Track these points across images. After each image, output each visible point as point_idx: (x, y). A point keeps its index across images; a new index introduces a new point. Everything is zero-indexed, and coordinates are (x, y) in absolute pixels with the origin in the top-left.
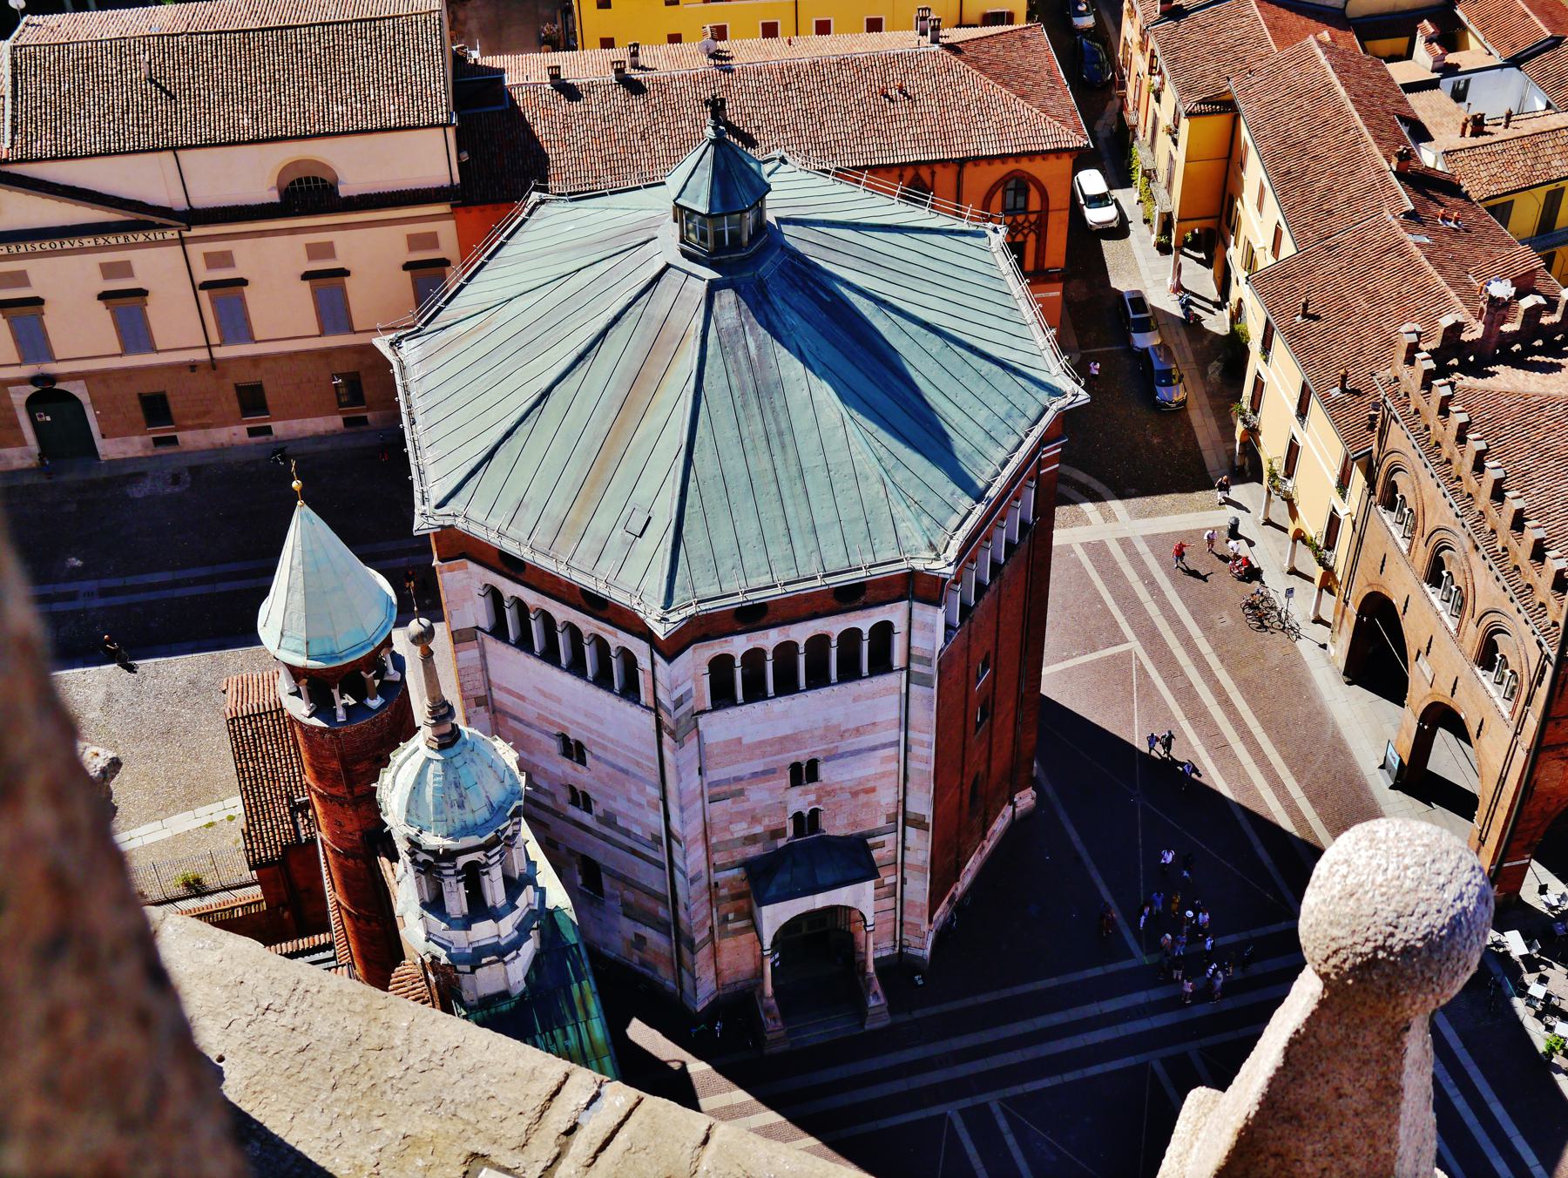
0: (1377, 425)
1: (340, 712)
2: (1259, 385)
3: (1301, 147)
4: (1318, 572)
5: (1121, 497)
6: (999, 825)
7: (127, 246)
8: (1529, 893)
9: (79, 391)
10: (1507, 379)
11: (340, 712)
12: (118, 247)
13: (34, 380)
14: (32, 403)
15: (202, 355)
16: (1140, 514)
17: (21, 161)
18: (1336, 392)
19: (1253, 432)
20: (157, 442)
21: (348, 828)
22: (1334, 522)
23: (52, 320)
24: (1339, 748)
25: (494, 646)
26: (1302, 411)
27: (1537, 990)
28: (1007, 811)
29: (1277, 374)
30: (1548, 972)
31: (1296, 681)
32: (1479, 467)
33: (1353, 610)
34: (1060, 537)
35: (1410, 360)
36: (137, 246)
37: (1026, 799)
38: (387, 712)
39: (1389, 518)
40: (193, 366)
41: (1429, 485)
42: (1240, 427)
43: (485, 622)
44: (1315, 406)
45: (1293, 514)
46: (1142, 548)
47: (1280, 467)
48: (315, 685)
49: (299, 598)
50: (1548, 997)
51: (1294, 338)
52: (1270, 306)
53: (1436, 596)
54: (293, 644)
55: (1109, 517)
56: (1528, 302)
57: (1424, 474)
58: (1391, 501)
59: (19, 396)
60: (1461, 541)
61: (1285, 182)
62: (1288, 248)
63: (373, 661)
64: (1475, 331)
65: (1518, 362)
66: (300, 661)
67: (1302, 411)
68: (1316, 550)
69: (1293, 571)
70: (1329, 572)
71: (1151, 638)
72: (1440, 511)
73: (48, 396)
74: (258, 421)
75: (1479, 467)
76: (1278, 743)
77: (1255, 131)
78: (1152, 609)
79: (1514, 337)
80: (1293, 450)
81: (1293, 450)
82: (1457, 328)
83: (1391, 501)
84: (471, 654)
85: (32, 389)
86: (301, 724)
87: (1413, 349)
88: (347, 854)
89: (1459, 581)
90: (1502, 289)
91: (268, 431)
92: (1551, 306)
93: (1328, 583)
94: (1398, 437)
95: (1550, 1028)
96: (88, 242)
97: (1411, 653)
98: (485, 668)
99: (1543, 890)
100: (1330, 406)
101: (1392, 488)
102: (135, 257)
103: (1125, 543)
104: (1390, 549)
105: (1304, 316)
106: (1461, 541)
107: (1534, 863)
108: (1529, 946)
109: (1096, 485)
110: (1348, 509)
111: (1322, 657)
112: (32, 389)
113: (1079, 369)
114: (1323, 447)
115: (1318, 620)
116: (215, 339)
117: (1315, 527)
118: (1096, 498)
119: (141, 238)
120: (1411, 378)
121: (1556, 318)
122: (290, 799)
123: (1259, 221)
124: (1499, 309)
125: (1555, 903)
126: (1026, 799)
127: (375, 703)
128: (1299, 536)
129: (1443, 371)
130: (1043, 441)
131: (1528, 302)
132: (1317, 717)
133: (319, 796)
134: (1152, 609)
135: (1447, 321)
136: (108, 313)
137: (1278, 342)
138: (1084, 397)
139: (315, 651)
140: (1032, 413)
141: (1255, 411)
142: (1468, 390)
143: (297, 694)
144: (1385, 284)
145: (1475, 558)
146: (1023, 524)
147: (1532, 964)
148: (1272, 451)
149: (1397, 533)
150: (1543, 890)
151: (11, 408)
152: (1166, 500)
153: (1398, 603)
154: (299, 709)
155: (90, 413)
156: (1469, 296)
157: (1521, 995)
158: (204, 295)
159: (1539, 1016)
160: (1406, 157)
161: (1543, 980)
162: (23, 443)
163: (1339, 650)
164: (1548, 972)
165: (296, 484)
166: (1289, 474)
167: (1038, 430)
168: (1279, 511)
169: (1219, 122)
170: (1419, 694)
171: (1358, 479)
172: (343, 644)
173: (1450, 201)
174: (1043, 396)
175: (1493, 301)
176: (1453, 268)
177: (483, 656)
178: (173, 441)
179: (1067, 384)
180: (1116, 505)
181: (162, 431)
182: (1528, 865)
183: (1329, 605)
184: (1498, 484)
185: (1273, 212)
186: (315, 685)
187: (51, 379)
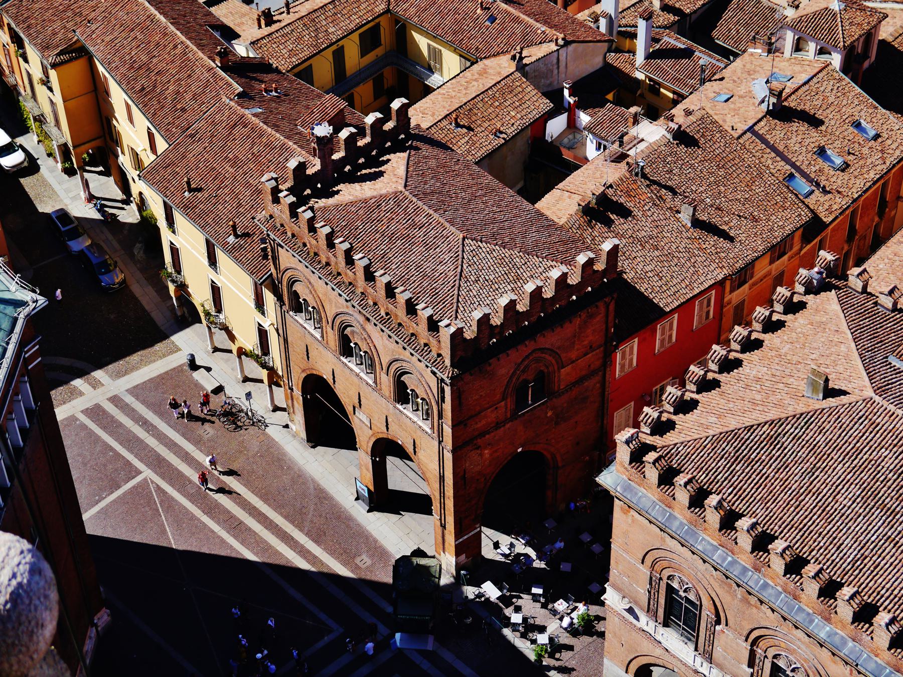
0: (269, 254)
2: (175, 251)
3: (146, 67)
4: (264, 374)
5: (100, 366)
6: (89, 646)
8: (488, 552)
10: (348, 192)
16: (119, 375)
18: (231, 239)
19: (182, 287)
22: (263, 334)
24: (322, 496)
26: (213, 261)
27: (516, 618)
28: (92, 632)
29: (185, 239)
30: (520, 602)
31: (275, 458)
32: (350, 262)
33: (298, 393)
34: (61, 413)
35: (276, 200)
37: (103, 618)
39: (300, 318)
41: (320, 285)
42: (172, 288)
44: (220, 255)
45: (232, 338)
46: (129, 399)
47: (210, 306)
50: (525, 619)
51: (188, 209)
52: (163, 191)
53: (351, 363)
55: (96, 385)
56: (344, 134)
57: (314, 279)
58: (297, 305)
60: (356, 318)
61: (145, 97)
62: (162, 145)
64: (315, 166)
65: (352, 178)
67: (213, 261)
68: (256, 358)
69: (246, 379)
70: (272, 371)
71: (158, 464)
72: (334, 302)
75: (350, 262)
76: (277, 508)
77: (107, 65)
78: (152, 442)
79: (343, 161)
80: (216, 291)
81: (216, 291)
82: (302, 166)
83: (297, 305)
87: (275, 191)
89: (364, 347)
90: (323, 130)
92: (361, 132)
93: (274, 380)
94: (286, 258)
95: (534, 642)
97: (349, 409)
99: (496, 545)
100: (231, 251)
101: (296, 295)
103: (115, 400)
104: (309, 340)
105: (191, 194)
106: (356, 318)
107: (484, 529)
108: (501, 589)
109: (78, 364)
110: (269, 321)
111: (288, 434)
113: (32, 280)
114: (236, 282)
115: (276, 409)
117: (250, 342)
118: (82, 373)
120: (281, 212)
121: (368, 139)
123: (134, 131)
124: (325, 145)
125: (508, 552)
126: (103, 618)
128: (241, 352)
129: (302, 201)
130: (22, 344)
131: (344, 134)
132: (299, 479)
134: (152, 442)
135: (292, 164)
137: (178, 217)
138: (42, 300)
140: (6, 325)
141: (179, 271)
142: (325, 209)
144: (240, 150)
145: (369, 327)
146: (29, 411)
147: (506, 600)
148: (200, 297)
149: (309, 326)
150: (496, 545)
152: (135, 358)
153: (328, 377)
156: (302, 141)
157: (507, 627)
159: (524, 636)
160: (225, 55)
161: (518, 609)
163: (298, 424)
164: (520, 602)
166: (219, 310)
167: (15, 337)
168: (221, 338)
169: (77, 67)
170: (365, 438)
171: (269, 298)
173: (267, 77)
174: (9, 310)
175: (320, 140)
176: (285, 125)
179: (26, 295)
180: (98, 374)
182: (480, 531)
183: (280, 394)
184: (367, 268)
185: (142, 122)
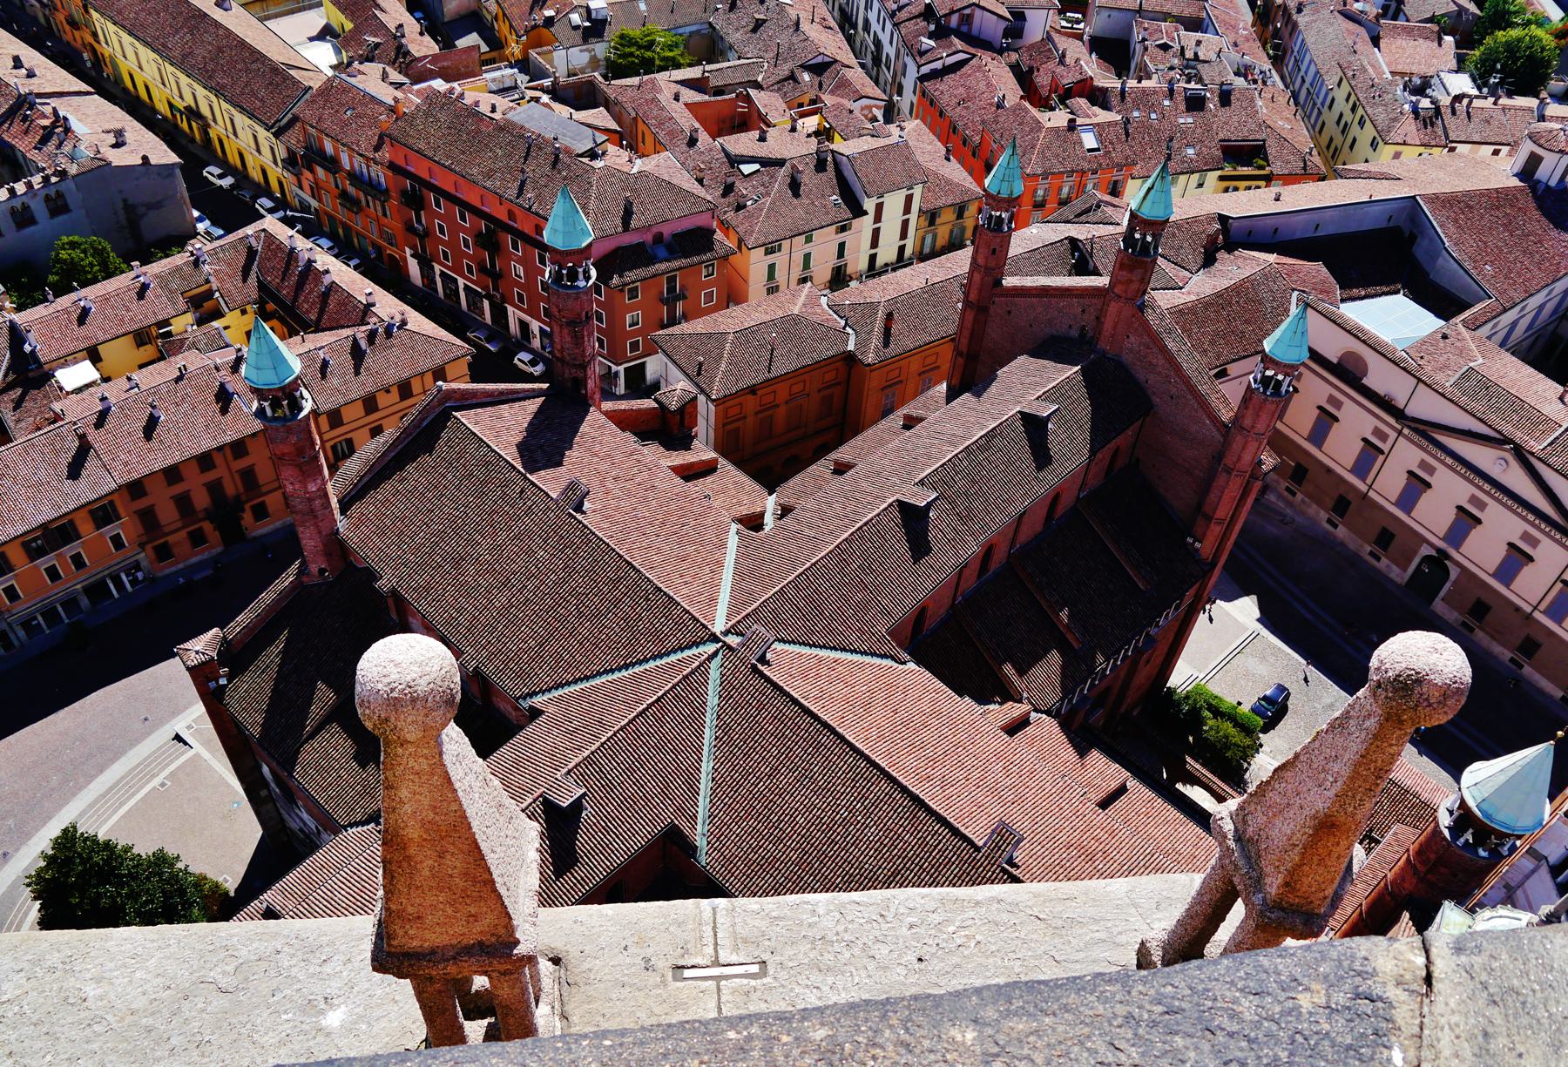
1: (1462, 840)
7: (1547, 535)
9: (1454, 573)
11: (1462, 840)
12: (1542, 531)
13: (1439, 550)
14: (1427, 559)
15: (1528, 609)
17: (1540, 459)
20: (1464, 624)
21: (1406, 885)
23: (1475, 535)
25: (1544, 872)
36: (1552, 538)
38: (1484, 863)
40: (1518, 609)
43: (1553, 859)
48: (1464, 819)
49: (1503, 779)
54: (1476, 793)
59: (1425, 551)
63: (1502, 836)
66: (1472, 804)
73: (1439, 562)
74: (1520, 658)
84: (1529, 864)
85: (1434, 553)
86: (1437, 825)
88: (1390, 894)
91: (1521, 667)
96: (1531, 517)
98: (1527, 877)
102: (1546, 543)
112: (1434, 553)
116: (1542, 607)
119: (1558, 536)
122: (1371, 830)
127: (1482, 853)
133: (1408, 859)
136: (1504, 553)
139: (1484, 806)
143: (1451, 813)
151: (1415, 553)
154: (1445, 820)
155: (1447, 586)
158: (1559, 585)
162: (1405, 569)
165: (1560, 733)
172: (1500, 817)
177: (1533, 871)
178: (1472, 630)
181: (1470, 621)
186: (1464, 819)
187: (1448, 557)
